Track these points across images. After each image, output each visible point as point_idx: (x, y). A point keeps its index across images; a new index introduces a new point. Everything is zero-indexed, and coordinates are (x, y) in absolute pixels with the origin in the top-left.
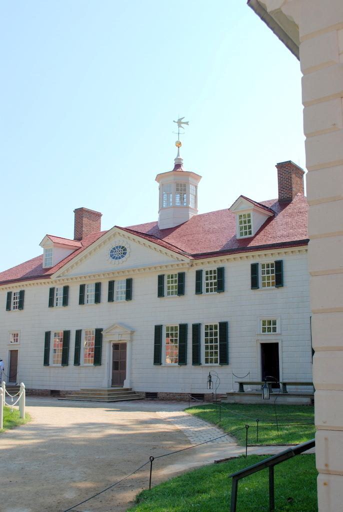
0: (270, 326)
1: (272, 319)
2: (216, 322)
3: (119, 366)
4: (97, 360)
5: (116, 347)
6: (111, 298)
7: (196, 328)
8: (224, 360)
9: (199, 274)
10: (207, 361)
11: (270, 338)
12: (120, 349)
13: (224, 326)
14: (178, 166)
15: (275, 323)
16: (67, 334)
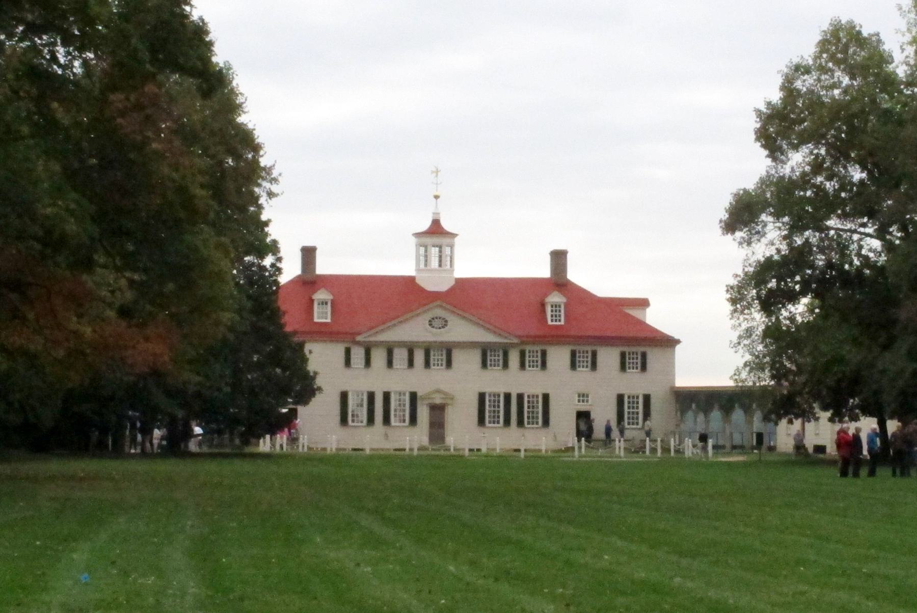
0: (583, 396)
1: (585, 392)
2: (539, 391)
3: (437, 427)
4: (413, 420)
6: (427, 364)
7: (520, 397)
8: (546, 422)
9: (522, 354)
10: (529, 423)
11: (583, 407)
12: (437, 410)
13: (546, 398)
14: (436, 223)
15: (587, 396)
16: (371, 396)
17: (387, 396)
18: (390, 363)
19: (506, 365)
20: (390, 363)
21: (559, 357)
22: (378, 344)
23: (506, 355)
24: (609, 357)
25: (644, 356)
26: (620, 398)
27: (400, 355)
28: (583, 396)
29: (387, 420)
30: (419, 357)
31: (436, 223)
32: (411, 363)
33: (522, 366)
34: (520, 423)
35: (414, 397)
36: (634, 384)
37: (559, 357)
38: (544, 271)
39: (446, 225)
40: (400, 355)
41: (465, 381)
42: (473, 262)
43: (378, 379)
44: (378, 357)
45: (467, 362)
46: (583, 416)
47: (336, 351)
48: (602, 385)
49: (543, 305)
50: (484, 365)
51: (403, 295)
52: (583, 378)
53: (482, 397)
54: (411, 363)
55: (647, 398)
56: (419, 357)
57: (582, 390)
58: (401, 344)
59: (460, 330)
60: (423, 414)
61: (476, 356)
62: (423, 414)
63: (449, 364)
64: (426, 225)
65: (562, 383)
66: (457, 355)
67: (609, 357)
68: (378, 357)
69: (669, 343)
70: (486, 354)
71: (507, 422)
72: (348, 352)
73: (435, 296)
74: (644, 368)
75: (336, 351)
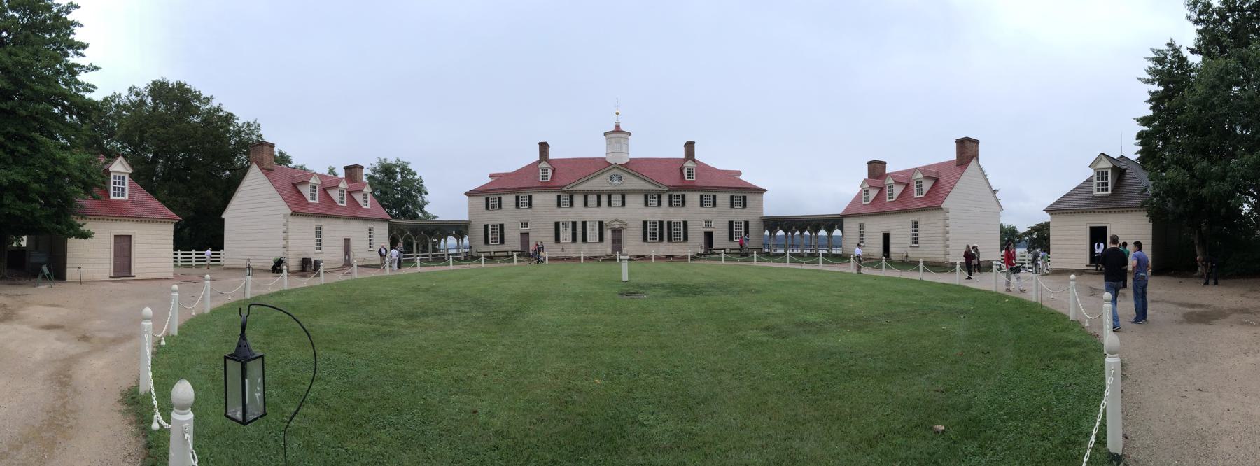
0: (708, 223)
2: (681, 220)
3: (617, 243)
4: (601, 239)
5: (614, 231)
6: (610, 204)
7: (669, 223)
8: (686, 239)
9: (670, 197)
11: (708, 229)
12: (617, 233)
13: (685, 223)
14: (618, 127)
16: (574, 224)
17: (584, 224)
18: (586, 204)
19: (660, 204)
20: (586, 204)
21: (693, 198)
22: (578, 192)
23: (660, 197)
24: (724, 199)
25: (745, 198)
26: (731, 223)
27: (592, 199)
28: (708, 223)
29: (584, 239)
30: (604, 199)
31: (618, 127)
32: (599, 204)
33: (670, 204)
34: (670, 239)
35: (601, 223)
36: (739, 215)
37: (693, 198)
38: (681, 154)
39: (623, 128)
40: (592, 199)
41: (635, 212)
42: (638, 149)
43: (578, 212)
44: (579, 200)
45: (635, 202)
46: (709, 236)
47: (552, 198)
48: (721, 215)
49: (681, 170)
50: (646, 204)
51: (600, 166)
52: (708, 212)
53: (645, 223)
54: (599, 204)
55: (747, 223)
56: (604, 199)
57: (708, 218)
58: (592, 192)
59: (630, 182)
60: (608, 235)
61: (641, 199)
62: (608, 235)
63: (623, 204)
64: (613, 128)
65: (693, 213)
66: (628, 198)
67: (724, 199)
68: (579, 200)
69: (761, 191)
70: (647, 195)
71: (661, 239)
72: (559, 197)
73: (617, 166)
74: (745, 206)
75: (552, 198)
